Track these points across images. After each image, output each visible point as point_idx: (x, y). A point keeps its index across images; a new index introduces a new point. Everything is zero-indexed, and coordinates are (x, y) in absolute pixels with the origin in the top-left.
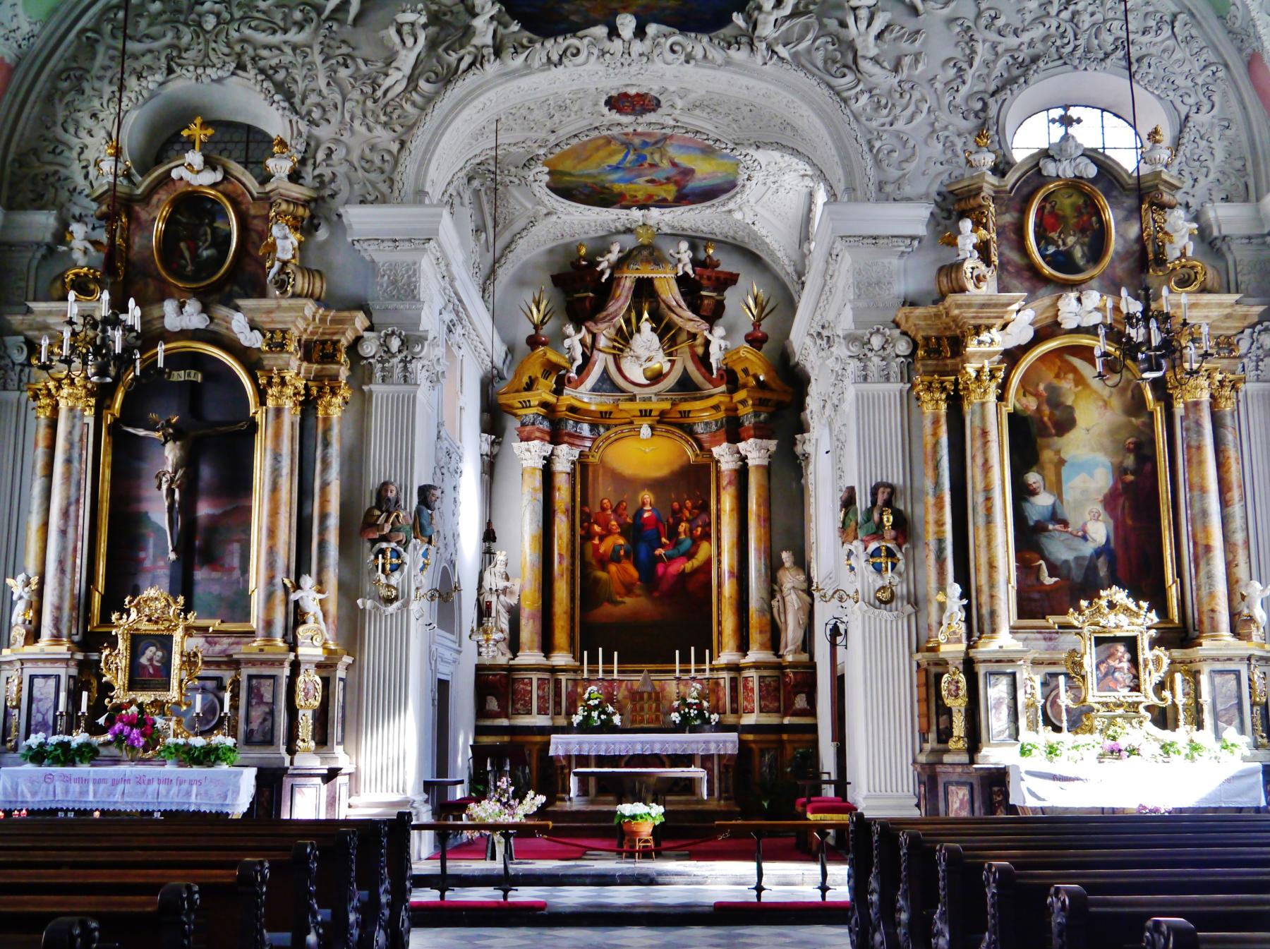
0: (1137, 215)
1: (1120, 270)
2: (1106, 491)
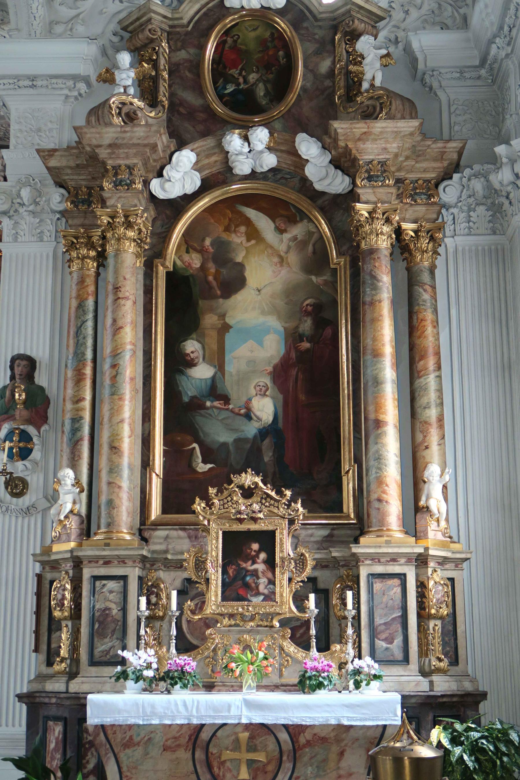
0: (329, 47)
1: (307, 109)
2: (276, 361)
